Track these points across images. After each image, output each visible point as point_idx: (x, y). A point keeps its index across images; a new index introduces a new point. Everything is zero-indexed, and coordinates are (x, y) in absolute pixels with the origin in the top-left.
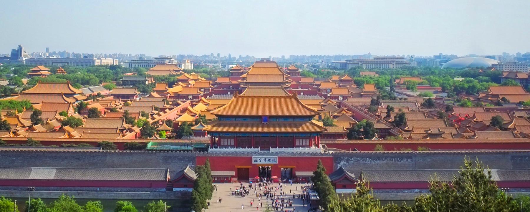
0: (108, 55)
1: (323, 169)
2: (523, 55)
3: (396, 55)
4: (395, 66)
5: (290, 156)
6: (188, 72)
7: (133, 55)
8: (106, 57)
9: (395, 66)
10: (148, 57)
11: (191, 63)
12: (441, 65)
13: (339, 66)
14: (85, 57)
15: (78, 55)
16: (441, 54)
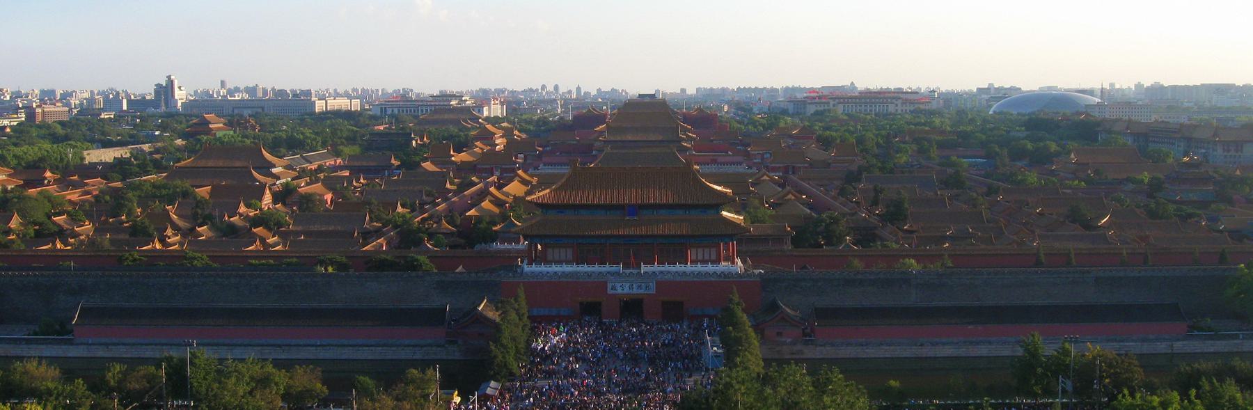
0: (341, 91)
1: (738, 304)
2: (1148, 88)
3: (905, 87)
4: (899, 108)
5: (678, 279)
6: (495, 121)
7: (390, 91)
8: (337, 95)
9: (899, 108)
10: (418, 95)
11: (502, 104)
12: (990, 106)
13: (791, 108)
14: (295, 95)
15: (282, 93)
16: (991, 85)
